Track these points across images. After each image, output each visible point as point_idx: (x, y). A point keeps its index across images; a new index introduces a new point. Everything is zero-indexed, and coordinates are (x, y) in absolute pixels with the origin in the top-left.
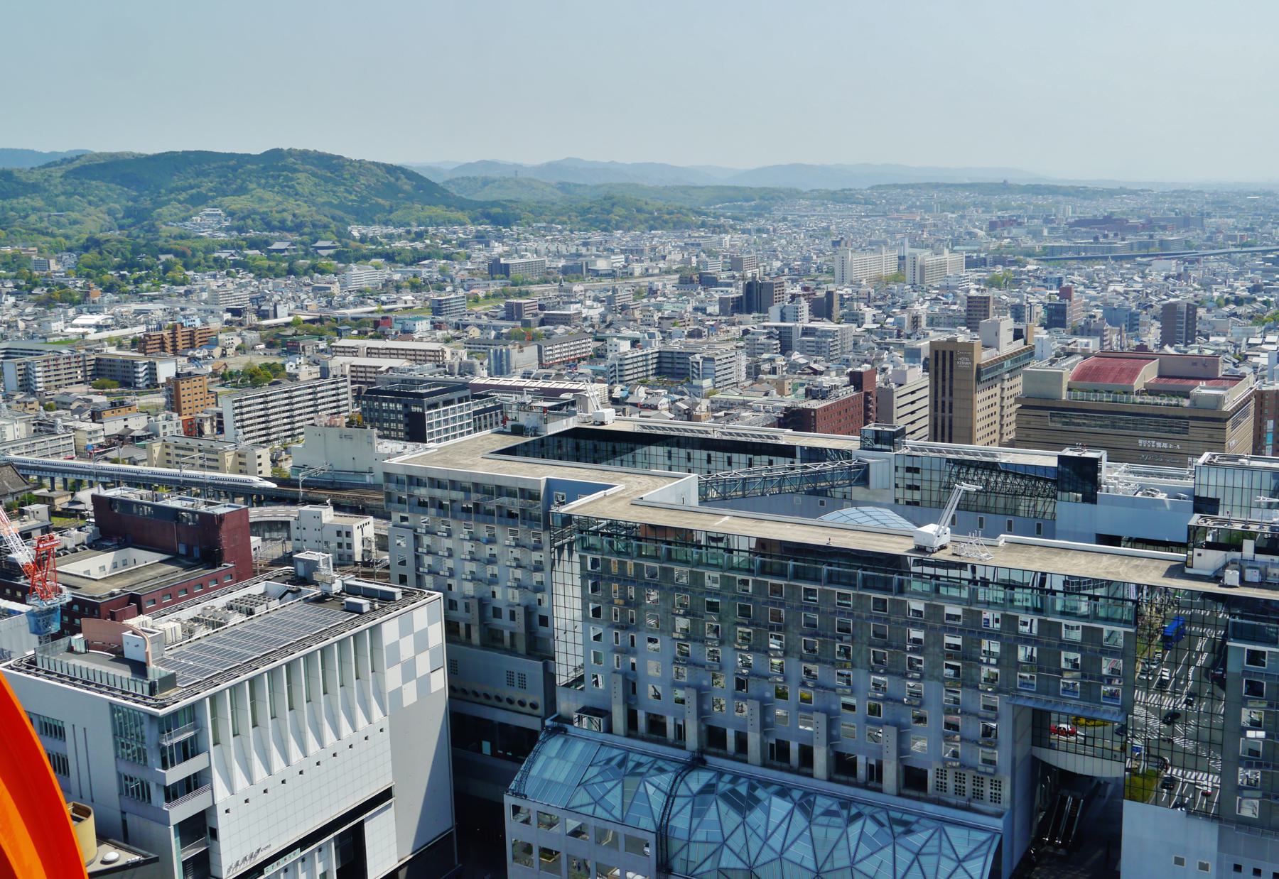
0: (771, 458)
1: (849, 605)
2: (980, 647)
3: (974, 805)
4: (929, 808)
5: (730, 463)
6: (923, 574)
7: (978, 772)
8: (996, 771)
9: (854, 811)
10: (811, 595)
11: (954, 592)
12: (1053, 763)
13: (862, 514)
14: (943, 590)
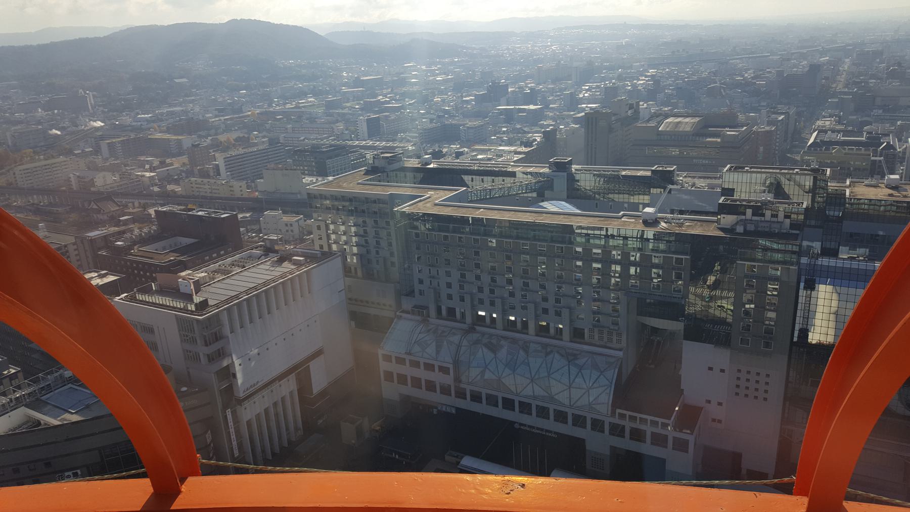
0: (504, 178)
1: (545, 250)
2: (611, 269)
3: (609, 345)
4: (586, 347)
5: (483, 181)
6: (581, 233)
7: (610, 329)
8: (619, 328)
9: (549, 350)
10: (525, 246)
11: (597, 242)
12: (647, 323)
13: (550, 205)
14: (591, 241)
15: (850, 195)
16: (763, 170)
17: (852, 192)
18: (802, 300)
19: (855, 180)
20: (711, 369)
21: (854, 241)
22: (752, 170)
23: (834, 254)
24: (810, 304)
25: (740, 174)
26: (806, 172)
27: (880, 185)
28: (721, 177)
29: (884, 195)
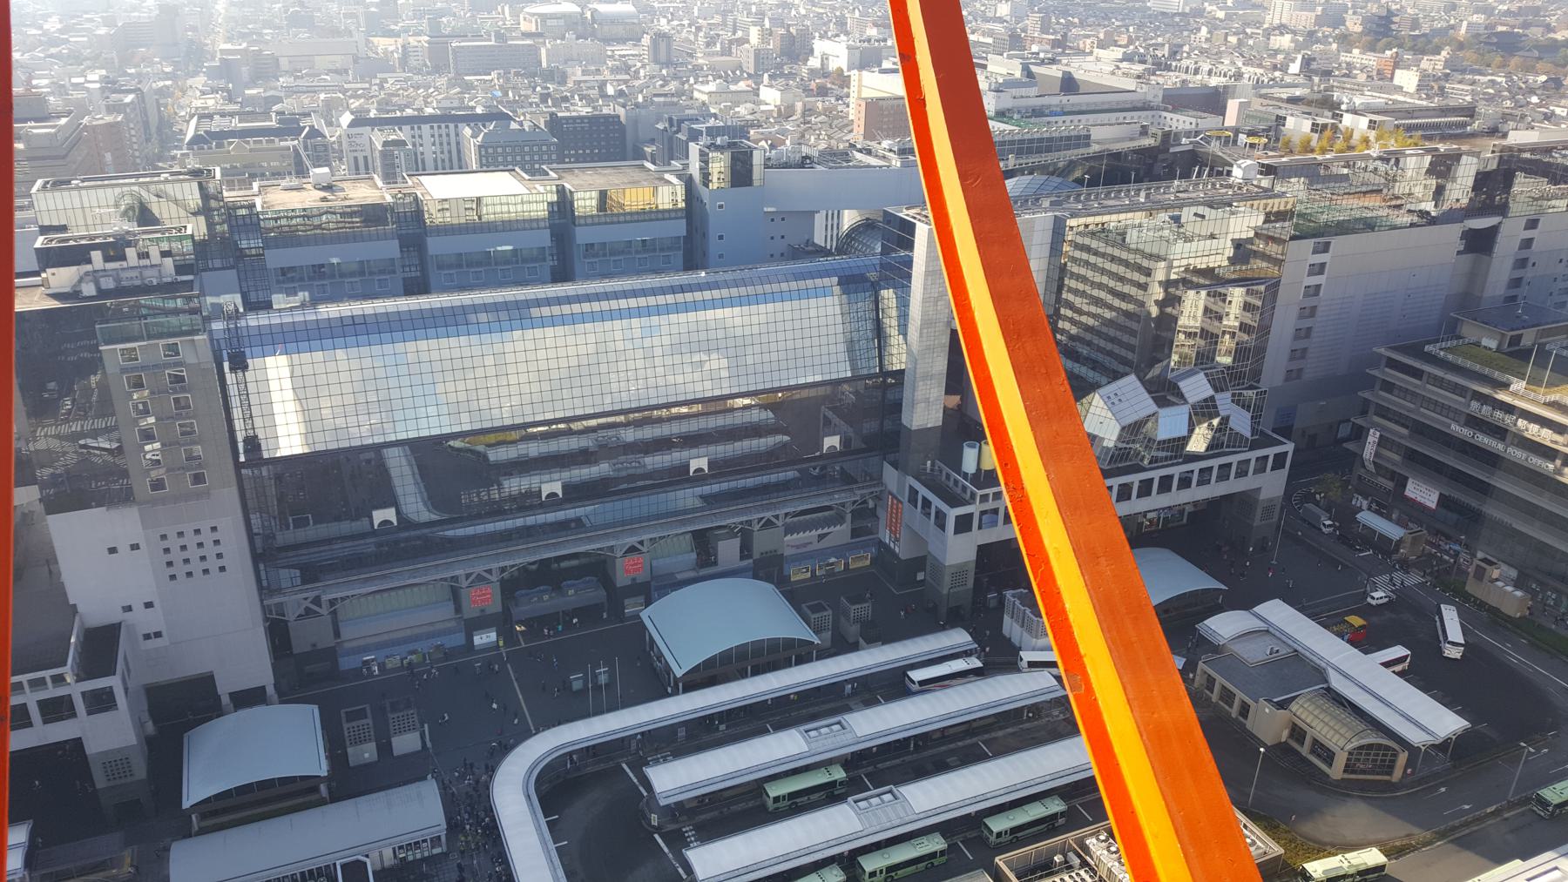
15: (263, 207)
16: (106, 182)
17: (265, 203)
18: (233, 390)
19: (266, 183)
20: (113, 550)
21: (289, 279)
22: (86, 184)
23: (267, 306)
24: (248, 394)
25: (66, 194)
26: (181, 177)
27: (304, 186)
28: (31, 205)
29: (314, 201)
